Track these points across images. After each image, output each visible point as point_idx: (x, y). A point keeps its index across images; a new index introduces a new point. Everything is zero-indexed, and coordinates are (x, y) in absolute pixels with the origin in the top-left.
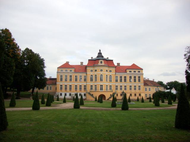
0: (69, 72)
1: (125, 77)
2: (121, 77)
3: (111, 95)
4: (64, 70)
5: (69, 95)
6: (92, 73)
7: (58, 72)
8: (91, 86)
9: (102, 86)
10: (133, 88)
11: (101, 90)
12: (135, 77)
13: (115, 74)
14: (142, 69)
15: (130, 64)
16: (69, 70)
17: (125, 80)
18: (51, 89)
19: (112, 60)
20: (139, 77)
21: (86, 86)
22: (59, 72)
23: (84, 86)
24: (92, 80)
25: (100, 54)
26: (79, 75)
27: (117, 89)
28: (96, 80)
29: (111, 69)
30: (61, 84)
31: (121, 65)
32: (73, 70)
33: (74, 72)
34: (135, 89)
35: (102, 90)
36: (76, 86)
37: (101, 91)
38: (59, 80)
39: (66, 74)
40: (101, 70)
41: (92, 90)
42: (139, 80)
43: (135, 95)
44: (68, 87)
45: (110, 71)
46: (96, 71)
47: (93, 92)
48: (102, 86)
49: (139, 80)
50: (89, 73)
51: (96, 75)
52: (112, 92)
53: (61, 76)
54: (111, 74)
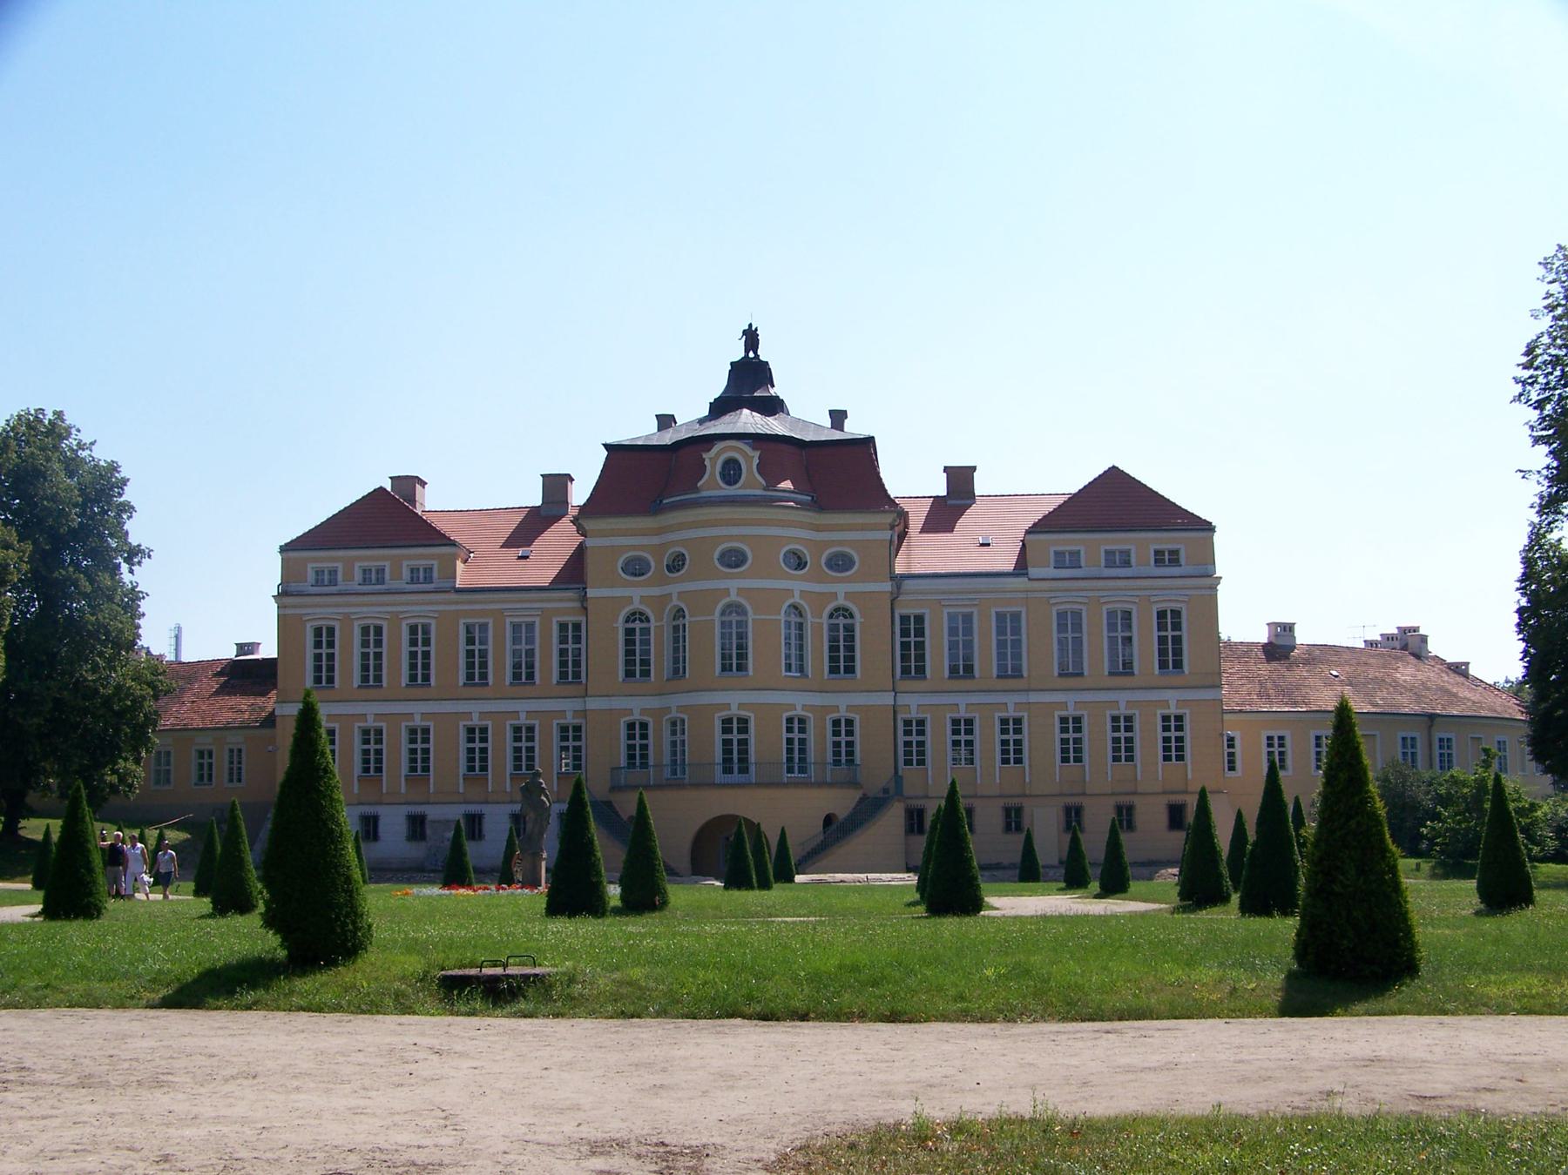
0: (396, 585)
3: (829, 820)
6: (637, 594)
7: (283, 595)
9: (743, 722)
11: (728, 770)
14: (1208, 528)
20: (1169, 619)
21: (577, 729)
22: (294, 587)
23: (564, 729)
24: (636, 666)
27: (915, 754)
28: (678, 672)
35: (744, 770)
37: (736, 777)
40: (734, 559)
45: (840, 563)
46: (676, 564)
47: (659, 786)
48: (743, 722)
52: (853, 783)
53: (324, 636)
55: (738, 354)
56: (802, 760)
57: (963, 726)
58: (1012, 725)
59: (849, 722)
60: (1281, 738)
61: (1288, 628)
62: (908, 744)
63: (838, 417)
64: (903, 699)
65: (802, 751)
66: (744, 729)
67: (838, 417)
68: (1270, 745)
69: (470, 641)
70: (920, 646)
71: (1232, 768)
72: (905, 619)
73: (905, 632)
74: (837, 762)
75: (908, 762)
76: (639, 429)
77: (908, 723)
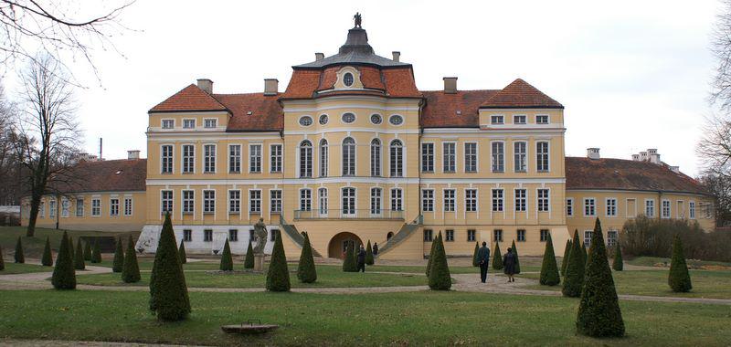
1: (471, 148)
2: (449, 148)
3: (390, 235)
4: (179, 121)
5: (202, 235)
6: (305, 133)
7: (150, 133)
8: (303, 192)
10: (509, 200)
11: (345, 212)
12: (520, 147)
13: (417, 131)
15: (499, 83)
16: (200, 120)
17: (471, 165)
18: (128, 211)
19: (410, 66)
20: (542, 147)
22: (154, 129)
25: (358, 34)
26: (248, 142)
27: (428, 206)
29: (399, 108)
30: (167, 184)
31: (461, 86)
32: (221, 120)
33: (224, 128)
34: (520, 206)
36: (235, 194)
38: (156, 168)
39: (189, 140)
41: (306, 214)
42: (543, 164)
43: (471, 235)
44: (199, 202)
45: (396, 120)
49: (543, 164)
50: (294, 130)
51: (324, 142)
53: (168, 150)
54: (396, 132)
55: (352, 26)
56: (378, 208)
57: (449, 193)
58: (471, 193)
59: (400, 191)
60: (592, 201)
61: (596, 150)
62: (425, 201)
63: (396, 54)
64: (423, 182)
65: (378, 204)
66: (352, 194)
67: (396, 54)
68: (587, 204)
69: (232, 153)
70: (431, 158)
71: (570, 214)
72: (425, 146)
73: (425, 152)
74: (394, 209)
75: (425, 209)
76: (308, 59)
77: (425, 192)
